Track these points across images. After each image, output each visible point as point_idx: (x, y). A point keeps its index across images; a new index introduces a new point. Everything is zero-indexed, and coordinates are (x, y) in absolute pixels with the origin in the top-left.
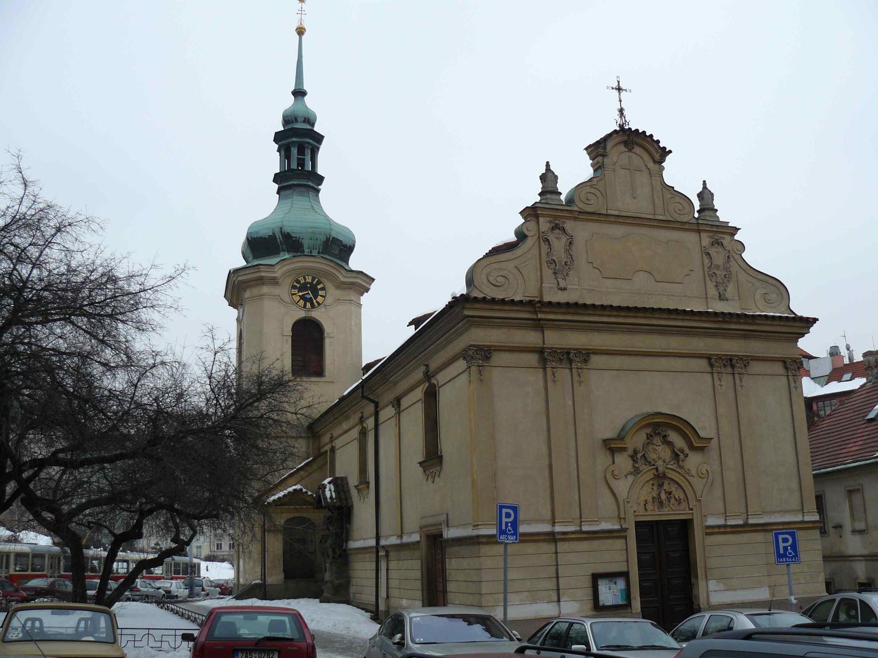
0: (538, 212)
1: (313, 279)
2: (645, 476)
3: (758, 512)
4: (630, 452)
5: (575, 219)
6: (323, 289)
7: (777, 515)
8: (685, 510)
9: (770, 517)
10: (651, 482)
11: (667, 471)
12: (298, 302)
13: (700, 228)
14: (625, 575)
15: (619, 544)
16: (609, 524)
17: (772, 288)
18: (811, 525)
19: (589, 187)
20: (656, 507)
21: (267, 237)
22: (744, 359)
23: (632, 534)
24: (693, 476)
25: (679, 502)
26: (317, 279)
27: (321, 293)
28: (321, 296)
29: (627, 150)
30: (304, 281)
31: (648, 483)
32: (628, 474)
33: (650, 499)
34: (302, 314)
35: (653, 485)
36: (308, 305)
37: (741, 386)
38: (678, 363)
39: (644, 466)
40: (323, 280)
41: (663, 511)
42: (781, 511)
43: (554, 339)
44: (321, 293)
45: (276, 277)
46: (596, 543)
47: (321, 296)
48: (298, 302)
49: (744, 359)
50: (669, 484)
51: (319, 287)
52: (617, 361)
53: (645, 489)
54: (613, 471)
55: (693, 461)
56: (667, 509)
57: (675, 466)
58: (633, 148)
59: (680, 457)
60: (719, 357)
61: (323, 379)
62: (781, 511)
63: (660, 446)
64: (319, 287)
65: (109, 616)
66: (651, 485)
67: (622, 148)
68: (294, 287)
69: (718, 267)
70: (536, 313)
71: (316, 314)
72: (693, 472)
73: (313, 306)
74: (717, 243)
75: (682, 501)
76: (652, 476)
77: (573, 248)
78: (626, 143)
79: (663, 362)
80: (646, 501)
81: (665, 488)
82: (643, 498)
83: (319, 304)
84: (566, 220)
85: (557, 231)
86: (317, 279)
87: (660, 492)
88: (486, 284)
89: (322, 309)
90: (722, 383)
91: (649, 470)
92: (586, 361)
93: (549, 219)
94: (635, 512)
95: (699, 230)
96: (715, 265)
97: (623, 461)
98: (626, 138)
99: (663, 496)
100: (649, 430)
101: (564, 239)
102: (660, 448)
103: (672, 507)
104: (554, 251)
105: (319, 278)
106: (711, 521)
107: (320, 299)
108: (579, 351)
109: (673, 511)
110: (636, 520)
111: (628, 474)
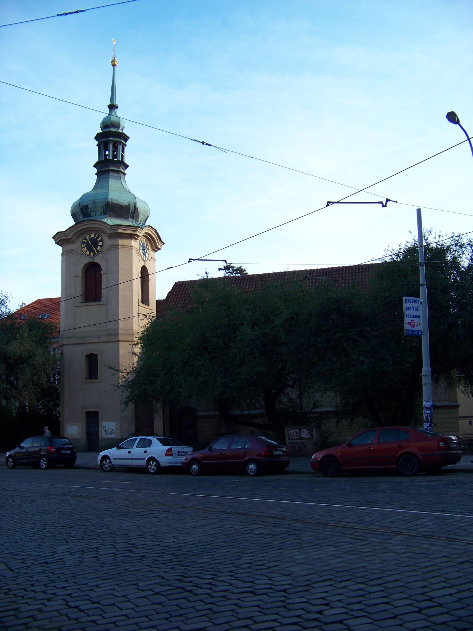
1: (95, 236)
6: (101, 241)
12: (85, 252)
21: (124, 205)
26: (97, 235)
27: (100, 244)
28: (100, 246)
34: (88, 260)
36: (92, 253)
40: (102, 235)
44: (100, 244)
47: (100, 246)
48: (85, 252)
51: (98, 240)
61: (101, 303)
64: (98, 240)
68: (83, 243)
71: (97, 260)
73: (94, 254)
83: (97, 251)
86: (97, 235)
89: (100, 255)
107: (99, 248)
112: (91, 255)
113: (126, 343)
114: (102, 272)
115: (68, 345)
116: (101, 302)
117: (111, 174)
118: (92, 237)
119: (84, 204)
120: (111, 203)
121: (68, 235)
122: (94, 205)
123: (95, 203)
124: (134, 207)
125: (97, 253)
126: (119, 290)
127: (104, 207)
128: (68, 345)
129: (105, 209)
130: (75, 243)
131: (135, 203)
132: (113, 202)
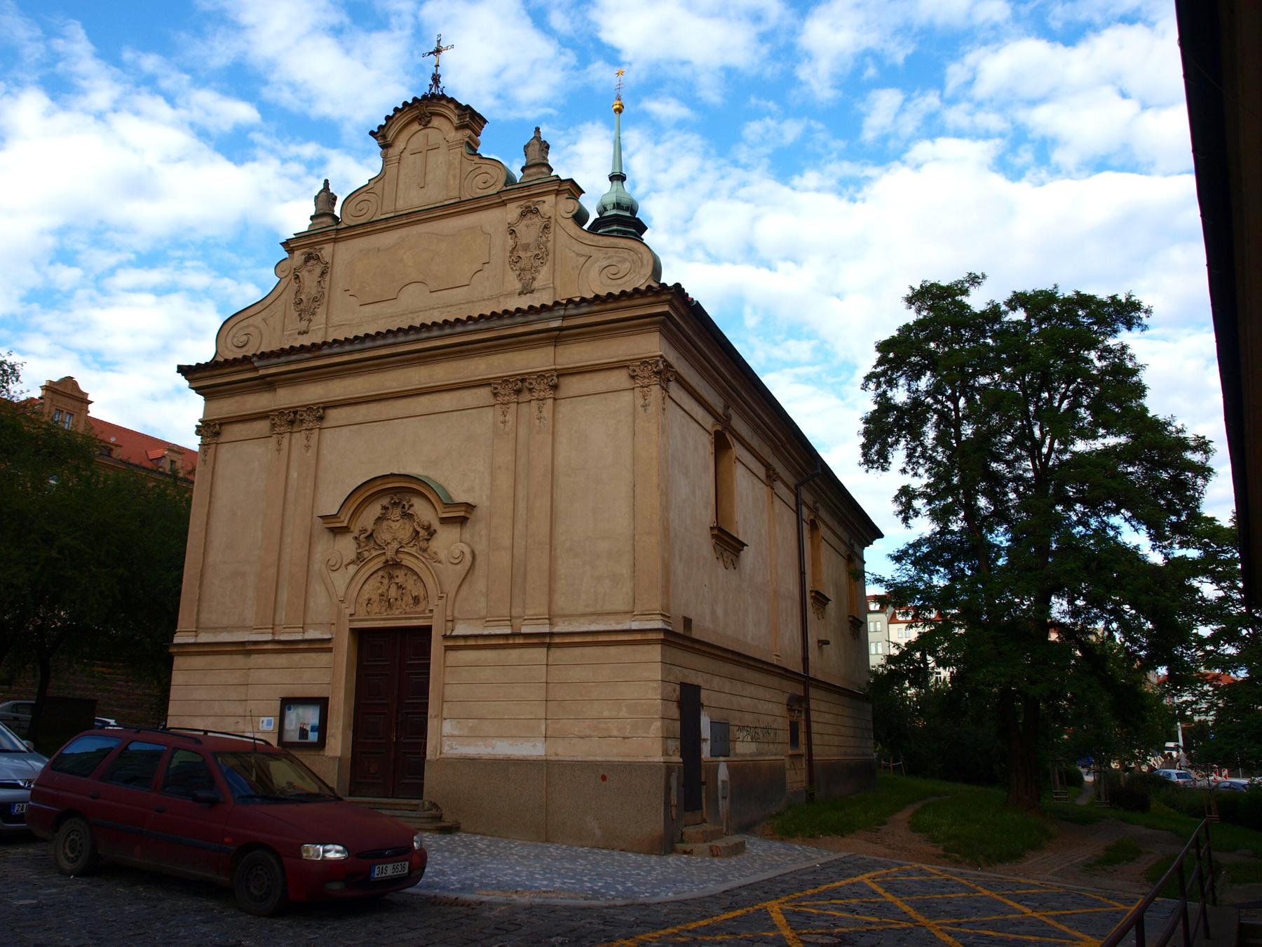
0: (291, 246)
2: (371, 564)
3: (544, 615)
4: (356, 533)
5: (335, 241)
7: (582, 620)
8: (423, 612)
9: (570, 624)
10: (381, 573)
11: (401, 556)
13: (503, 198)
14: (322, 703)
15: (324, 658)
16: (319, 632)
17: (625, 254)
18: (639, 637)
19: (364, 194)
20: (383, 609)
22: (547, 375)
23: (344, 644)
24: (440, 562)
25: (416, 600)
29: (421, 127)
31: (375, 575)
32: (349, 564)
33: (375, 597)
35: (383, 577)
37: (539, 419)
38: (447, 401)
39: (372, 551)
41: (393, 614)
42: (593, 614)
43: (285, 397)
46: (296, 657)
49: (547, 375)
50: (406, 575)
52: (362, 412)
53: (371, 582)
54: (329, 560)
55: (447, 541)
56: (397, 612)
57: (415, 548)
58: (429, 122)
59: (420, 535)
60: (505, 380)
62: (593, 614)
63: (398, 520)
65: (133, 743)
66: (379, 578)
67: (416, 127)
69: (526, 247)
70: (256, 369)
72: (442, 555)
74: (527, 212)
75: (421, 600)
76: (380, 565)
77: (327, 277)
78: (416, 119)
79: (424, 403)
80: (370, 600)
81: (397, 580)
82: (366, 597)
84: (325, 246)
85: (312, 262)
87: (390, 587)
88: (230, 348)
90: (507, 418)
91: (377, 556)
92: (321, 418)
93: (305, 250)
94: (351, 615)
95: (503, 201)
96: (522, 245)
97: (346, 546)
98: (416, 112)
99: (393, 592)
100: (385, 501)
101: (318, 270)
102: (398, 524)
103: (408, 609)
104: (303, 289)
106: (461, 630)
108: (309, 408)
109: (406, 613)
110: (351, 627)
111: (349, 564)
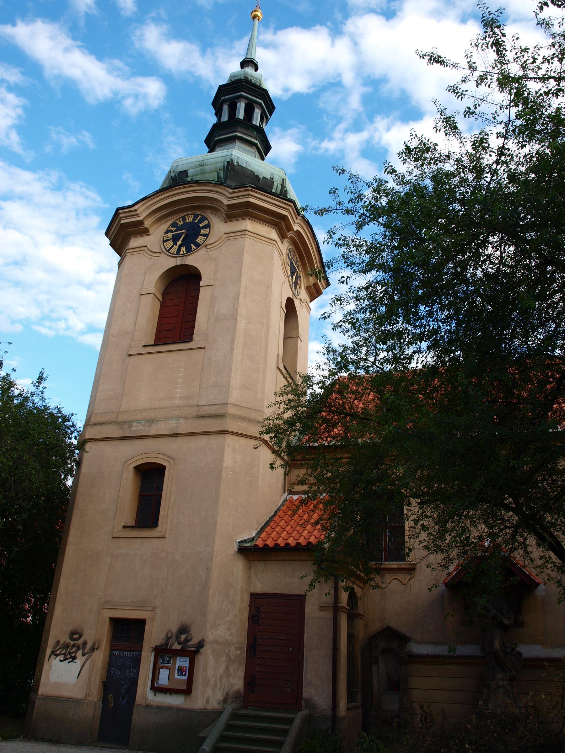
1: (194, 219)
26: (200, 216)
30: (182, 223)
34: (172, 262)
44: (202, 232)
45: (141, 222)
51: (201, 225)
64: (201, 225)
71: (192, 260)
105: (202, 213)
112: (181, 253)
113: (243, 440)
114: (202, 283)
115: (96, 440)
116: (191, 343)
117: (238, 143)
118: (188, 221)
119: (180, 169)
120: (235, 164)
121: (138, 214)
122: (200, 168)
123: (201, 165)
124: (280, 187)
125: (195, 248)
126: (239, 318)
127: (222, 172)
128: (96, 440)
129: (222, 175)
130: (150, 235)
131: (283, 179)
132: (240, 164)
